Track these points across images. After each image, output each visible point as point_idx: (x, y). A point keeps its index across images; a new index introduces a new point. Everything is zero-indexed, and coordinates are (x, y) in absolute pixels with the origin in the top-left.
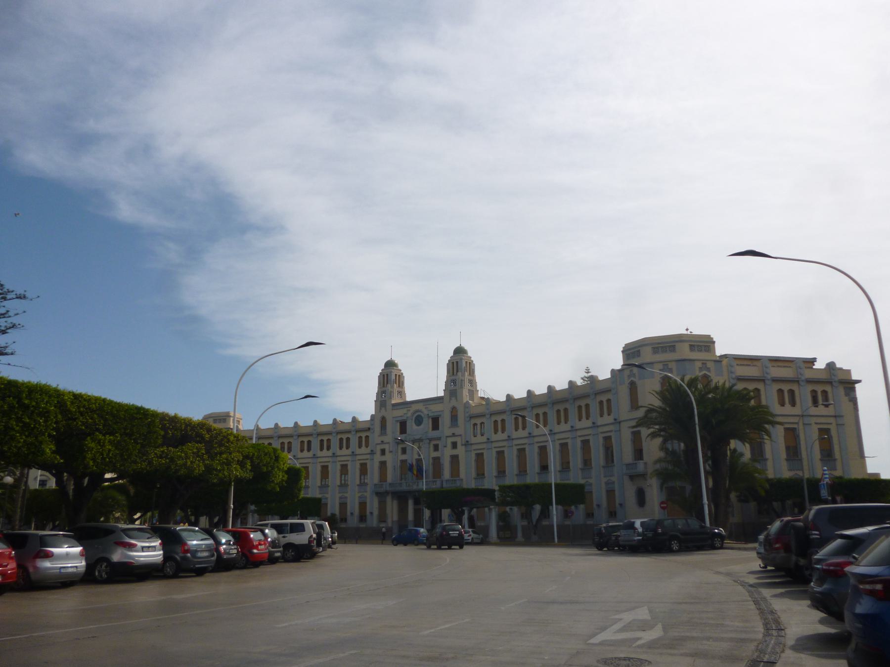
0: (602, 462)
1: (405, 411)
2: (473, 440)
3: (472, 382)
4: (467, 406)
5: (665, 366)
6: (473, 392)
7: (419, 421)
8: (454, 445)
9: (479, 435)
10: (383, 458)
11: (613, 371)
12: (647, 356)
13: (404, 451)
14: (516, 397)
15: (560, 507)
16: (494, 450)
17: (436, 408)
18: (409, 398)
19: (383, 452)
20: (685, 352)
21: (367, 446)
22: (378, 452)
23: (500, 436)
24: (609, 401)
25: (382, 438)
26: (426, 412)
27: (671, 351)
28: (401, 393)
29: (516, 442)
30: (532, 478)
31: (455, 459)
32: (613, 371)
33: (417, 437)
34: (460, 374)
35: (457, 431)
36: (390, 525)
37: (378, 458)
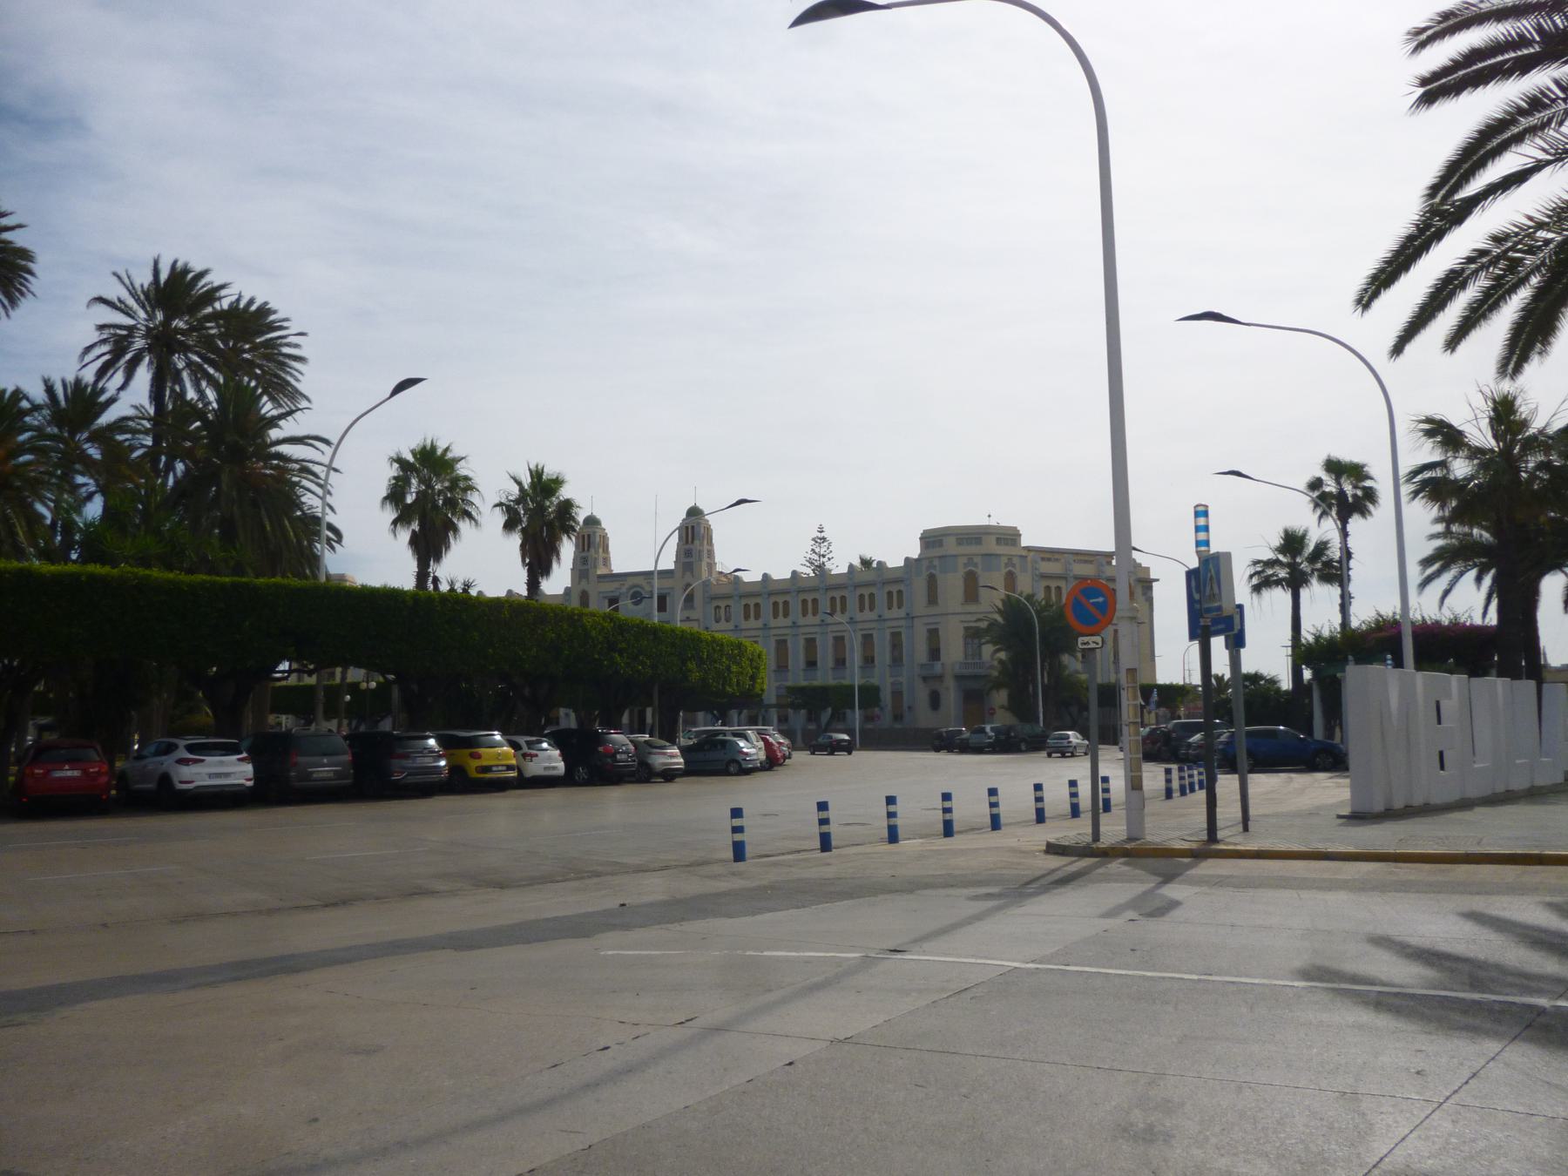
0: (888, 658)
1: (616, 585)
3: (711, 554)
4: (706, 584)
5: (970, 558)
6: (711, 565)
7: (638, 597)
11: (907, 560)
12: (951, 547)
14: (775, 577)
18: (616, 571)
20: (991, 546)
24: (900, 592)
28: (606, 561)
32: (907, 560)
34: (697, 542)
35: (694, 615)
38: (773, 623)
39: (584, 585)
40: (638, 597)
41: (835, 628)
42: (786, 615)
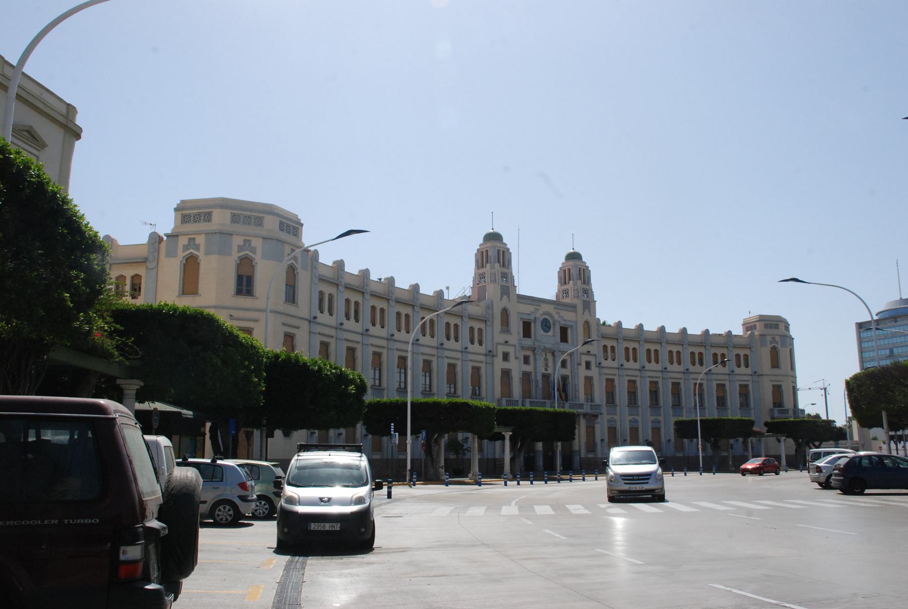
2: (605, 363)
7: (546, 325)
8: (588, 365)
9: (610, 359)
10: (506, 365)
13: (526, 360)
16: (648, 380)
17: (568, 317)
19: (506, 357)
21: (481, 343)
22: (500, 356)
25: (506, 337)
26: (556, 317)
31: (589, 380)
33: (548, 346)
37: (499, 364)
39: (505, 302)
40: (546, 325)
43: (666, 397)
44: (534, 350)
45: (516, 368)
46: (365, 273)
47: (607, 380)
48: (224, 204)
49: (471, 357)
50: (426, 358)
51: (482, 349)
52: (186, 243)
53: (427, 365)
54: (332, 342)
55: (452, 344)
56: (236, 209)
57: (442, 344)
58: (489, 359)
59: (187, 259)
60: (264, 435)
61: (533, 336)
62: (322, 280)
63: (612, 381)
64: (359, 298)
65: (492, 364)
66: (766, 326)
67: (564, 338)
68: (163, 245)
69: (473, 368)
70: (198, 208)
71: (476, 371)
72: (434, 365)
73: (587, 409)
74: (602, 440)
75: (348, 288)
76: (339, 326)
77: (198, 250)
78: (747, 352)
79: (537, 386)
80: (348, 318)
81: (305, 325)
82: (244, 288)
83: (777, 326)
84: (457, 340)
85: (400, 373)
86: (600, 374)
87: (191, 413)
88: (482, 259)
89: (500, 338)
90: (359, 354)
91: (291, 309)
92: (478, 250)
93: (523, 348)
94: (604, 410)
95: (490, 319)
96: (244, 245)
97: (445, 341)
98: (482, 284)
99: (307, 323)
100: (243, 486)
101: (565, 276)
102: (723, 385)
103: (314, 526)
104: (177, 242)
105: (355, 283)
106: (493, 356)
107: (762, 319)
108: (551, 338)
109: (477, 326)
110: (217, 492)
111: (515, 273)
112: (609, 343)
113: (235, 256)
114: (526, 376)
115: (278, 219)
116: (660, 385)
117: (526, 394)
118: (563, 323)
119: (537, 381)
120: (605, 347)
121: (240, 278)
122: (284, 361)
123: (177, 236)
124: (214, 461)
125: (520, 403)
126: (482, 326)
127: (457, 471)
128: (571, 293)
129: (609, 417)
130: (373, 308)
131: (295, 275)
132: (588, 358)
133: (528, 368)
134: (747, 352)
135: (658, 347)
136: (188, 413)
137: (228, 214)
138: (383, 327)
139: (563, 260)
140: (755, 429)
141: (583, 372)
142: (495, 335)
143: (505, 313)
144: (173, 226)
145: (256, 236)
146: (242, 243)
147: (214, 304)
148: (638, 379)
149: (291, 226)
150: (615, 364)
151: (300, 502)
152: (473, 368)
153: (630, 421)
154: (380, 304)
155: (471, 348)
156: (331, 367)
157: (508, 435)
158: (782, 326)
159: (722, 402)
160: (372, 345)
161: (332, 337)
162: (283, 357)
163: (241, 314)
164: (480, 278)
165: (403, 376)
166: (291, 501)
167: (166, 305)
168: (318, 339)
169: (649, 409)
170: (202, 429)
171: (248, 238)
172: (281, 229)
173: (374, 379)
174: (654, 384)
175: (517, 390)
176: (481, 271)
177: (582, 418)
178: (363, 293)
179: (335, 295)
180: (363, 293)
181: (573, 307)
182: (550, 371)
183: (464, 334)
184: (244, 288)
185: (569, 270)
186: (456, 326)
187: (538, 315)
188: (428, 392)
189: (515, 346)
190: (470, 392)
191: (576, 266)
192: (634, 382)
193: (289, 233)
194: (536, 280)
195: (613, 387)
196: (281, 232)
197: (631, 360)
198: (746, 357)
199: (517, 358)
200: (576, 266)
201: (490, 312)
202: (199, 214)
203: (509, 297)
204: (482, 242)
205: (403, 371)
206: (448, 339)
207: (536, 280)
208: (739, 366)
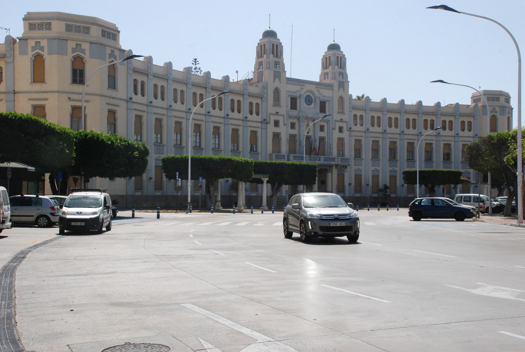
1: (298, 88)
2: (354, 128)
7: (309, 100)
8: (341, 130)
9: (358, 125)
10: (277, 130)
13: (293, 126)
15: (193, 181)
16: (388, 141)
19: (277, 123)
21: (258, 114)
22: (272, 123)
23: (376, 129)
26: (317, 94)
27: (497, 100)
29: (407, 137)
30: (438, 165)
31: (341, 141)
33: (309, 116)
35: (345, 118)
36: (284, 195)
37: (272, 129)
38: (406, 131)
39: (277, 84)
40: (309, 100)
41: (373, 135)
42: (451, 129)
43: (402, 153)
44: (298, 118)
45: (285, 131)
46: (169, 65)
47: (356, 140)
48: (60, 17)
49: (250, 124)
50: (216, 125)
51: (259, 118)
52: (34, 45)
53: (216, 130)
54: (145, 115)
55: (236, 115)
56: (68, 21)
57: (228, 115)
58: (264, 126)
59: (35, 57)
60: (83, 181)
61: (298, 108)
62: (136, 71)
63: (360, 141)
64: (164, 84)
65: (266, 129)
66: (489, 99)
67: (323, 109)
68: (17, 46)
69: (252, 132)
70: (41, 19)
71: (254, 134)
72: (222, 130)
73: (338, 161)
74: (350, 184)
75: (155, 76)
76: (149, 104)
77: (43, 51)
78: (471, 119)
79: (300, 145)
80: (156, 97)
81: (123, 104)
82: (78, 79)
83: (498, 99)
84: (239, 112)
85: (196, 136)
86: (350, 136)
87: (34, 168)
88: (261, 50)
89: (272, 110)
90: (164, 123)
91: (112, 93)
92: (259, 44)
93: (290, 117)
94: (352, 162)
95: (265, 96)
96: (77, 47)
97: (230, 113)
98: (260, 70)
99: (125, 102)
100: (53, 208)
101: (326, 63)
102: (449, 145)
103: (73, 224)
104: (27, 44)
105: (161, 72)
106: (267, 123)
107: (487, 93)
108: (313, 110)
109: (255, 101)
110: (39, 212)
111: (285, 62)
112: (359, 113)
113: (70, 55)
114: (292, 138)
115: (100, 29)
116: (398, 144)
117: (292, 150)
118: (322, 98)
119: (300, 142)
120: (355, 116)
121: (74, 72)
122: (90, 138)
123: (27, 39)
124: (37, 196)
125: (286, 157)
126: (259, 101)
127: (229, 204)
128: (330, 75)
129: (356, 167)
130: (175, 90)
131: (115, 69)
132: (341, 124)
133: (294, 132)
134: (471, 119)
135: (398, 116)
136: (31, 169)
137: (63, 24)
138: (183, 103)
139: (326, 50)
140: (462, 178)
141: (336, 134)
142: (269, 107)
143: (277, 92)
144: (22, 31)
145: (85, 41)
146: (75, 47)
147: (56, 89)
148: (380, 140)
149: (111, 33)
150: (363, 129)
151: (68, 214)
152: (252, 132)
153: (373, 171)
154: (180, 87)
155: (250, 117)
156: (121, 140)
157: (265, 180)
158: (502, 99)
159: (447, 157)
160: (174, 116)
161: (144, 111)
162: (90, 136)
163: (76, 97)
164: (259, 65)
165: (198, 137)
166: (64, 213)
167: (11, 113)
168: (133, 114)
169: (388, 162)
170: (42, 178)
171: (79, 43)
172: (103, 36)
173: (177, 140)
174: (393, 144)
175: (284, 148)
176: (260, 60)
177: (334, 168)
178: (167, 80)
179: (146, 82)
180: (167, 80)
181: (330, 87)
182: (311, 134)
183: (245, 108)
184: (78, 79)
185: (330, 57)
186: (239, 102)
187: (302, 92)
188: (217, 150)
189: (283, 116)
190: (249, 149)
191: (334, 55)
192: (377, 142)
193: (109, 38)
194: (303, 65)
195: (361, 145)
196: (103, 38)
197: (376, 126)
198: (470, 123)
199: (285, 124)
200: (334, 55)
201: (265, 91)
202: (42, 24)
203: (280, 80)
204: (261, 37)
205: (198, 134)
206: (233, 111)
207: (303, 65)
208: (463, 130)
